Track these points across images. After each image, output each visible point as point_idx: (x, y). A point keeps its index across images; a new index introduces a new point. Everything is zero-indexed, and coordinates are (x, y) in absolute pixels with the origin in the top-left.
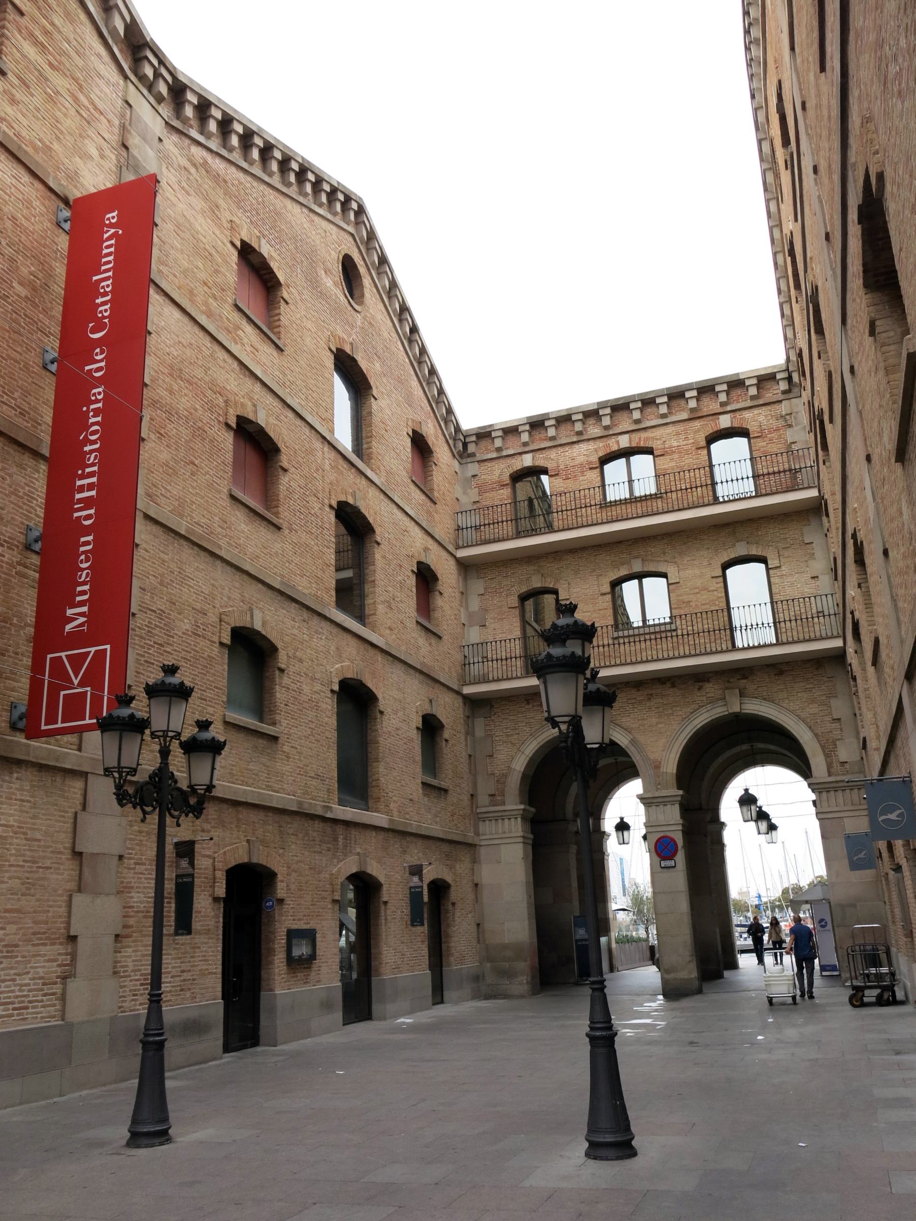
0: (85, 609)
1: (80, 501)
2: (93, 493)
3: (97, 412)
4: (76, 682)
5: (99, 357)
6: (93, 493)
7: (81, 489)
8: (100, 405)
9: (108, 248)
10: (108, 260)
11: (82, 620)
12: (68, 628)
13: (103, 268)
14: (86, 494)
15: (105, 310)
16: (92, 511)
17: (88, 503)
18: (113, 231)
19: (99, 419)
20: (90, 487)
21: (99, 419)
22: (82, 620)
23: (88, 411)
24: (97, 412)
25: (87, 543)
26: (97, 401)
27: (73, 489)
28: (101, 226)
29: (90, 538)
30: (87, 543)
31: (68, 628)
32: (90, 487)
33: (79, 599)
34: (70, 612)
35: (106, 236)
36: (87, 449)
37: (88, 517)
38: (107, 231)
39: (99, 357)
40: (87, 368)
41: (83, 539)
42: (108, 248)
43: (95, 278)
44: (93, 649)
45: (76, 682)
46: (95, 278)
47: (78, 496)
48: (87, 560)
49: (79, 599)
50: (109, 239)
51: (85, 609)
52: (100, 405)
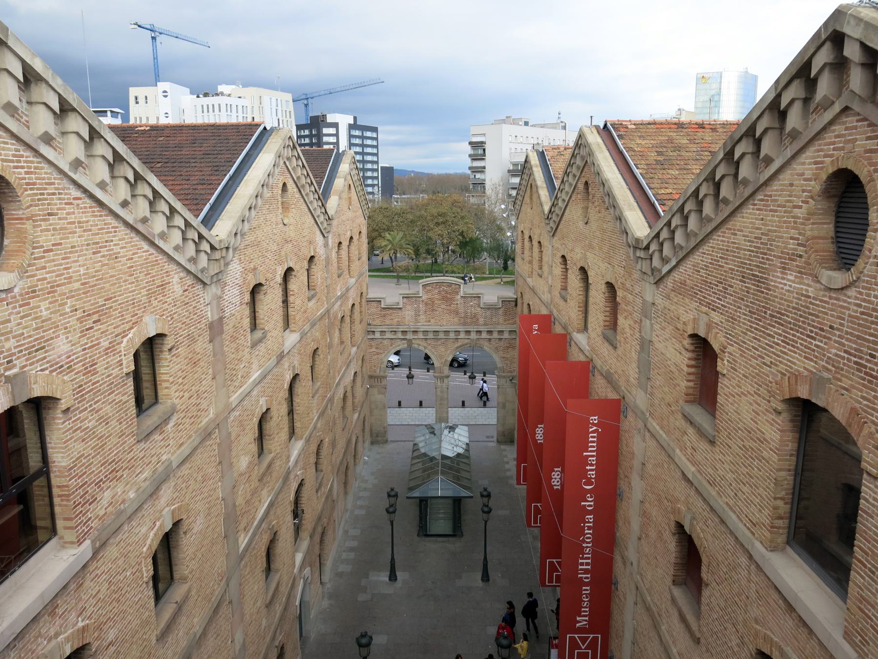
0: (587, 618)
1: (581, 570)
2: (589, 567)
3: (589, 528)
4: (583, 648)
5: (590, 499)
6: (589, 567)
7: (582, 564)
8: (591, 525)
9: (593, 438)
10: (593, 446)
11: (585, 623)
12: (578, 625)
13: (590, 449)
14: (585, 567)
15: (592, 474)
16: (589, 576)
17: (586, 571)
18: (595, 428)
19: (591, 532)
20: (587, 564)
21: (591, 532)
22: (585, 623)
23: (584, 526)
24: (589, 528)
25: (587, 590)
26: (589, 522)
27: (577, 564)
28: (587, 424)
29: (588, 588)
30: (587, 590)
31: (578, 625)
32: (587, 564)
33: (583, 613)
34: (578, 619)
35: (591, 430)
36: (584, 545)
37: (586, 578)
38: (591, 428)
39: (590, 499)
40: (582, 503)
41: (584, 588)
42: (593, 438)
43: (585, 454)
44: (592, 636)
45: (583, 648)
46: (585, 454)
47: (580, 567)
48: (587, 597)
49: (583, 613)
50: (593, 432)
51: (587, 618)
52: (591, 525)
